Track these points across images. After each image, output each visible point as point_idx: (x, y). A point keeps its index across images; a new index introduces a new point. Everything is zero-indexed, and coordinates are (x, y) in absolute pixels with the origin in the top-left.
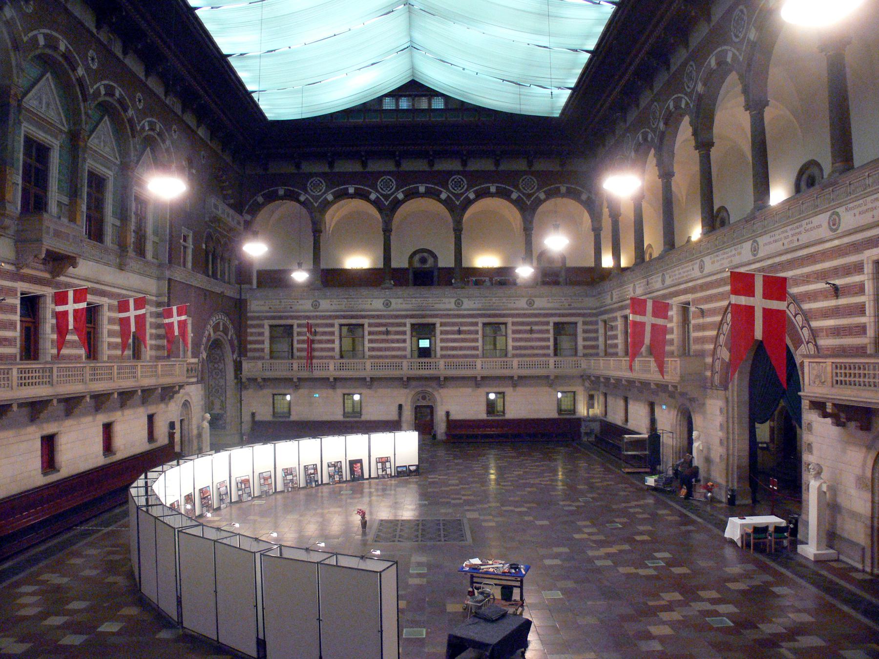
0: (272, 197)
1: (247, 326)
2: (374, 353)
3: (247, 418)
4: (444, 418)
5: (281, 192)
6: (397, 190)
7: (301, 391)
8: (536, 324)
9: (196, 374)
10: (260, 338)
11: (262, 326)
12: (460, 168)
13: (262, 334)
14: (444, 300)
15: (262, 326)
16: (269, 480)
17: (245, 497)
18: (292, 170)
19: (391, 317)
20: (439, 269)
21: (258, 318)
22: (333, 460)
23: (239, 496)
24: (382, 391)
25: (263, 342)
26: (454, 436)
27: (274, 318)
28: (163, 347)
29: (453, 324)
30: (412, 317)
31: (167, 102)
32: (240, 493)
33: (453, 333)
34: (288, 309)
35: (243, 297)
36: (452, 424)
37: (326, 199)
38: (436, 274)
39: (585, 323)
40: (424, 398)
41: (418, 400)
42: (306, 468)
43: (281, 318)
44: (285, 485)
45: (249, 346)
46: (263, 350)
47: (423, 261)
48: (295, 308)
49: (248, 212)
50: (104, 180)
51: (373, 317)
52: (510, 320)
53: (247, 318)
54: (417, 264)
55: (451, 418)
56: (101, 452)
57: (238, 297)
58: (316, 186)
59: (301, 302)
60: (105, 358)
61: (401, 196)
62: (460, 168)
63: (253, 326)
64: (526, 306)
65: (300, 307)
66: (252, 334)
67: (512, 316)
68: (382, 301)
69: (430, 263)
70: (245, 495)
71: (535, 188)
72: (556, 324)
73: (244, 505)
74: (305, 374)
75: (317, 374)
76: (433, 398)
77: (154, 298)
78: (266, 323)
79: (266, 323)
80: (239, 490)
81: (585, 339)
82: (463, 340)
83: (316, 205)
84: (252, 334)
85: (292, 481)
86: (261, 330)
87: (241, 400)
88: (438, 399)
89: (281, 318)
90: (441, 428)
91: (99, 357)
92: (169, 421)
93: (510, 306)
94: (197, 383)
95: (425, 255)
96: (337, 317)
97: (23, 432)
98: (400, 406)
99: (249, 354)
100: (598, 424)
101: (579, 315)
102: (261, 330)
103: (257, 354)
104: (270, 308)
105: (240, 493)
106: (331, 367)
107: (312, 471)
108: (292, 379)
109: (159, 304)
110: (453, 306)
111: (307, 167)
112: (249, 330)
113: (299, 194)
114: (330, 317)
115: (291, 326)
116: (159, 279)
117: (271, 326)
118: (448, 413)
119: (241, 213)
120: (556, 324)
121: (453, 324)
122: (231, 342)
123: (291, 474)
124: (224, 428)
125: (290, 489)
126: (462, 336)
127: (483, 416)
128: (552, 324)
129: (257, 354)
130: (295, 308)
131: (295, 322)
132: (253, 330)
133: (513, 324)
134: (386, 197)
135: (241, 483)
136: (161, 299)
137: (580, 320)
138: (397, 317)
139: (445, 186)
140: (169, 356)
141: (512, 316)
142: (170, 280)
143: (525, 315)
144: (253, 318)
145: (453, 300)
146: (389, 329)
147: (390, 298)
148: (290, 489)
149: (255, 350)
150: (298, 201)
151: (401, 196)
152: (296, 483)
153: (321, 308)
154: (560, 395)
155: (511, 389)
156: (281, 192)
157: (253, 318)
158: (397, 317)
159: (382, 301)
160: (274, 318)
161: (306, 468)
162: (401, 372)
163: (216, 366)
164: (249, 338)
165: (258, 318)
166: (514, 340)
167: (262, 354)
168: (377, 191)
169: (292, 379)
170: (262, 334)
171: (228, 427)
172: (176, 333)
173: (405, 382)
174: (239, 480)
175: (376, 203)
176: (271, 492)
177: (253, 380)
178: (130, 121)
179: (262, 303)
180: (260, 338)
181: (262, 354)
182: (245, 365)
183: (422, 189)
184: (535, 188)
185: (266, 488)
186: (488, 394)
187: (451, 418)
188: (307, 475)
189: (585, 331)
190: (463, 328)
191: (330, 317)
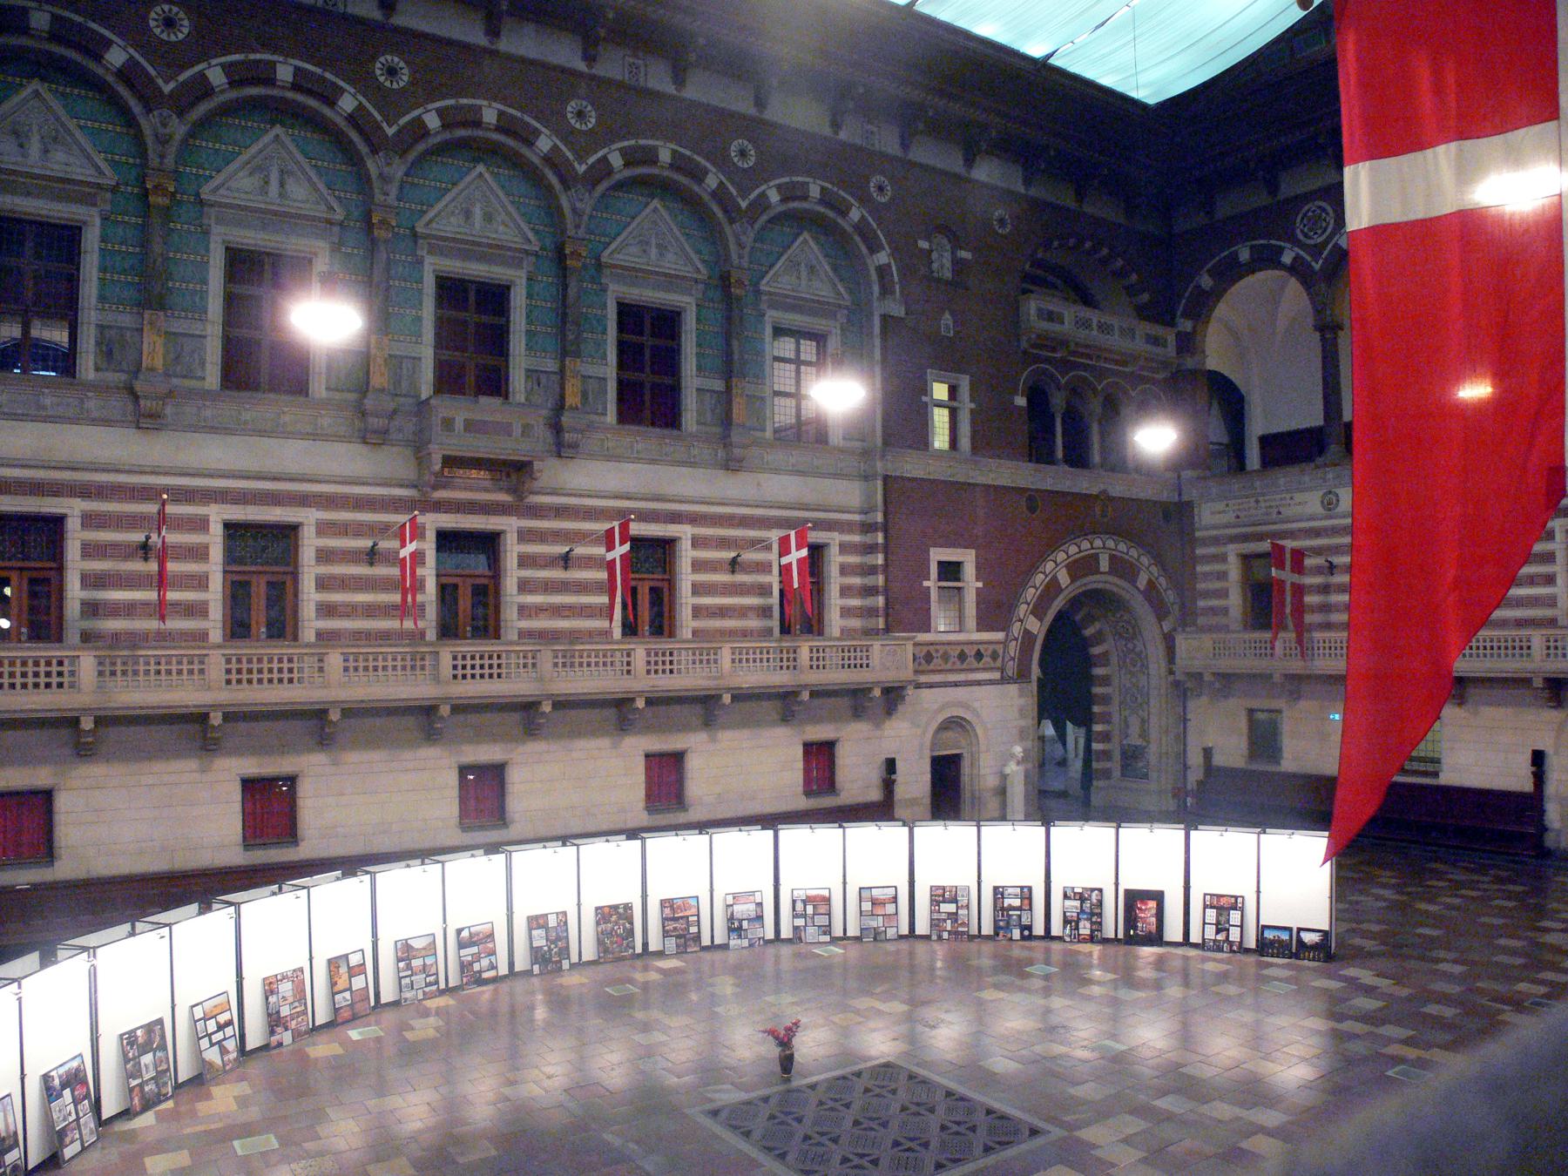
0: (1230, 273)
3: (1195, 759)
5: (1244, 255)
7: (1304, 704)
9: (999, 663)
10: (1218, 585)
11: (1223, 558)
15: (1223, 558)
16: (890, 909)
17: (811, 934)
18: (1260, 199)
21: (1216, 541)
22: (1080, 883)
23: (796, 928)
24: (1489, 713)
25: (1223, 594)
28: (877, 610)
31: (843, 135)
32: (800, 922)
35: (1185, 498)
37: (1336, 245)
42: (998, 893)
44: (935, 924)
45: (1201, 603)
49: (1187, 314)
50: (679, 314)
53: (1194, 541)
56: (642, 804)
57: (1176, 499)
59: (1299, 497)
60: (836, 633)
65: (1297, 510)
66: (1206, 575)
70: (810, 930)
73: (802, 948)
74: (1296, 666)
77: (857, 517)
79: (1233, 551)
80: (795, 916)
83: (1317, 266)
85: (953, 916)
86: (1218, 567)
87: (1185, 720)
91: (827, 630)
92: (884, 757)
94: (1004, 680)
97: (407, 755)
98: (891, 765)
99: (1201, 621)
102: (1218, 567)
103: (1214, 620)
104: (1238, 517)
105: (800, 922)
107: (1017, 902)
108: (1271, 676)
109: (867, 528)
113: (1280, 251)
116: (866, 478)
119: (1170, 323)
122: (1151, 591)
123: (954, 900)
124: (1146, 776)
125: (945, 935)
129: (1214, 620)
132: (1207, 568)
135: (805, 902)
136: (869, 519)
140: (887, 630)
142: (886, 478)
144: (1205, 542)
148: (945, 935)
149: (1213, 611)
150: (1279, 265)
152: (963, 924)
156: (1244, 255)
157: (1205, 542)
160: (1245, 538)
161: (998, 893)
162: (1529, 666)
163: (1130, 646)
165: (1216, 541)
167: (1223, 621)
169: (1271, 676)
171: (1154, 775)
172: (796, 585)
174: (801, 894)
176: (891, 933)
177: (1198, 677)
178: (720, 195)
179: (1220, 506)
180: (1218, 585)
181: (1223, 621)
182: (1182, 643)
185: (878, 922)
188: (1000, 908)
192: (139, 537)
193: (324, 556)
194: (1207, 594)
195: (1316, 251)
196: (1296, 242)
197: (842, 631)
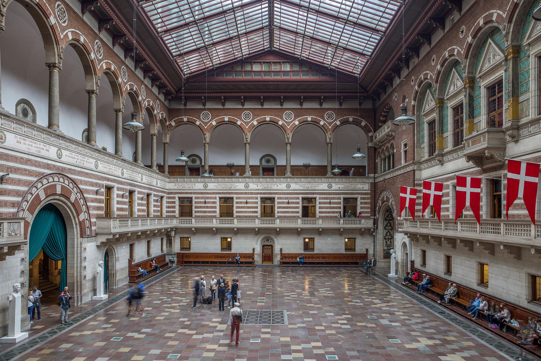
4: (279, 253)
6: (253, 120)
8: (334, 198)
19: (249, 193)
20: (277, 166)
26: (284, 263)
30: (261, 193)
34: (191, 188)
36: (283, 256)
38: (275, 169)
39: (361, 198)
40: (268, 240)
41: (264, 242)
46: (174, 212)
47: (268, 161)
51: (237, 193)
52: (318, 196)
54: (264, 163)
55: (283, 252)
58: (206, 116)
64: (327, 188)
69: (272, 164)
71: (334, 119)
72: (344, 199)
76: (273, 240)
78: (177, 196)
81: (362, 208)
82: (290, 208)
88: (276, 242)
90: (277, 259)
93: (317, 188)
95: (268, 157)
101: (359, 194)
114: (214, 193)
115: (192, 198)
117: (179, 198)
118: (281, 250)
120: (344, 199)
126: (290, 205)
128: (342, 199)
133: (320, 198)
134: (247, 123)
137: (360, 196)
138: (252, 193)
143: (326, 194)
146: (248, 201)
147: (249, 182)
153: (208, 188)
154: (346, 240)
158: (252, 193)
166: (320, 208)
184: (334, 119)
186: (305, 239)
187: (283, 252)
189: (361, 203)
190: (290, 201)
191: (214, 193)
193: (320, 203)
195: (206, 124)
197: (166, 216)
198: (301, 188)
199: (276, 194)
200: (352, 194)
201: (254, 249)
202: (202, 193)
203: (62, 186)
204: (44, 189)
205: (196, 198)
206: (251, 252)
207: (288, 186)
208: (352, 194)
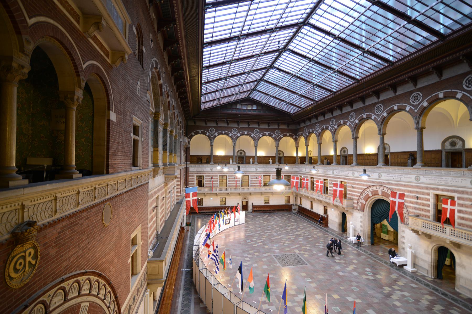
0: (197, 133)
1: (188, 176)
2: (230, 185)
4: (251, 205)
5: (200, 132)
6: (238, 133)
11: (194, 176)
12: (258, 127)
13: (194, 179)
14: (252, 168)
15: (194, 176)
18: (204, 125)
21: (192, 173)
25: (194, 181)
26: (255, 211)
27: (198, 173)
29: (255, 176)
33: (254, 178)
36: (254, 207)
40: (245, 198)
43: (200, 173)
48: (205, 170)
53: (189, 173)
55: (254, 205)
59: (207, 168)
61: (239, 135)
62: (258, 127)
63: (191, 176)
66: (190, 179)
67: (272, 173)
68: (233, 168)
75: (214, 192)
78: (195, 175)
84: (190, 179)
86: (193, 177)
88: (250, 199)
89: (200, 173)
96: (219, 173)
99: (189, 185)
100: (298, 207)
101: (292, 173)
102: (193, 177)
106: (218, 190)
110: (254, 170)
111: (209, 124)
112: (189, 177)
121: (255, 176)
127: (263, 204)
130: (205, 170)
131: (205, 175)
134: (235, 135)
139: (253, 133)
141: (272, 173)
144: (190, 173)
145: (255, 168)
151: (239, 135)
153: (213, 170)
155: (271, 195)
157: (190, 173)
159: (233, 168)
160: (198, 173)
164: (189, 180)
165: (192, 173)
168: (232, 133)
170: (194, 179)
173: (239, 194)
175: (231, 137)
179: (194, 168)
183: (246, 133)
192: (256, 177)
194: (190, 181)
195: (212, 135)
196: (209, 132)
198: (262, 170)
199: (249, 173)
200: (288, 173)
201: (238, 204)
202: (209, 173)
203: (382, 191)
204: (371, 192)
205: (206, 176)
206: (237, 205)
207: (256, 169)
208: (288, 173)
